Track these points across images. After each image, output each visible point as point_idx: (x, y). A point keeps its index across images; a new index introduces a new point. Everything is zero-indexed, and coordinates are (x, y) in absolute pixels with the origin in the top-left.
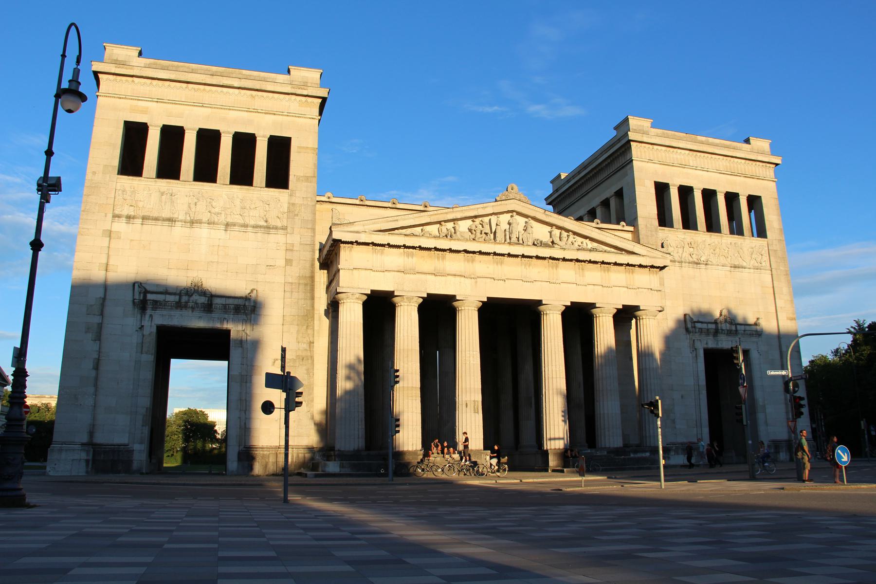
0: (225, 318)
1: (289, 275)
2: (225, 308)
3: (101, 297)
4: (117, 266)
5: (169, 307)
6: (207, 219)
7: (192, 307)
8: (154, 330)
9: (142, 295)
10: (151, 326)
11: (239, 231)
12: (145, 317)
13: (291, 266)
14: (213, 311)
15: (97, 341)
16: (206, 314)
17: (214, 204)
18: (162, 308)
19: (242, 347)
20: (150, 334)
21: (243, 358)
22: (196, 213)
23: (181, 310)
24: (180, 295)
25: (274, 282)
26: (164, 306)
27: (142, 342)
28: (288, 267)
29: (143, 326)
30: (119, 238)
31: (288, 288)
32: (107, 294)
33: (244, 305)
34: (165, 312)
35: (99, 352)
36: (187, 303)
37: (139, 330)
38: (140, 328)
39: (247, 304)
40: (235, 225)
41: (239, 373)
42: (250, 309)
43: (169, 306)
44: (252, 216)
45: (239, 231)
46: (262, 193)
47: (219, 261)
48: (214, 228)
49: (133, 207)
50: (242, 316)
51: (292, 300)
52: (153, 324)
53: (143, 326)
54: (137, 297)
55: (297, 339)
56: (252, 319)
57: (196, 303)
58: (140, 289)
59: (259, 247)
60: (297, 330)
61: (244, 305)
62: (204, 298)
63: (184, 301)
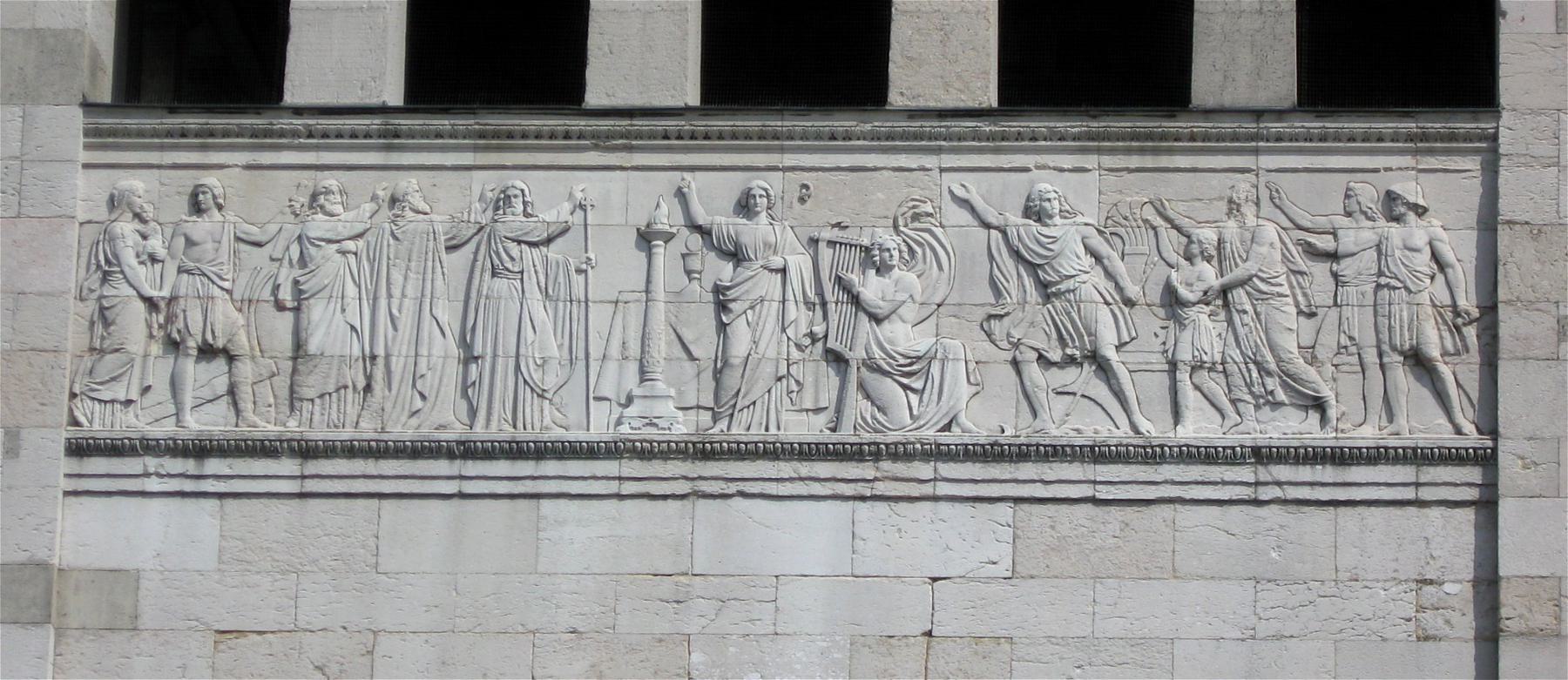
6: (821, 420)
11: (1094, 501)
17: (872, 288)
22: (732, 380)
40: (1055, 453)
44: (1196, 367)
45: (1094, 501)
46: (1267, 161)
48: (881, 488)
49: (220, 364)
59: (1263, 629)
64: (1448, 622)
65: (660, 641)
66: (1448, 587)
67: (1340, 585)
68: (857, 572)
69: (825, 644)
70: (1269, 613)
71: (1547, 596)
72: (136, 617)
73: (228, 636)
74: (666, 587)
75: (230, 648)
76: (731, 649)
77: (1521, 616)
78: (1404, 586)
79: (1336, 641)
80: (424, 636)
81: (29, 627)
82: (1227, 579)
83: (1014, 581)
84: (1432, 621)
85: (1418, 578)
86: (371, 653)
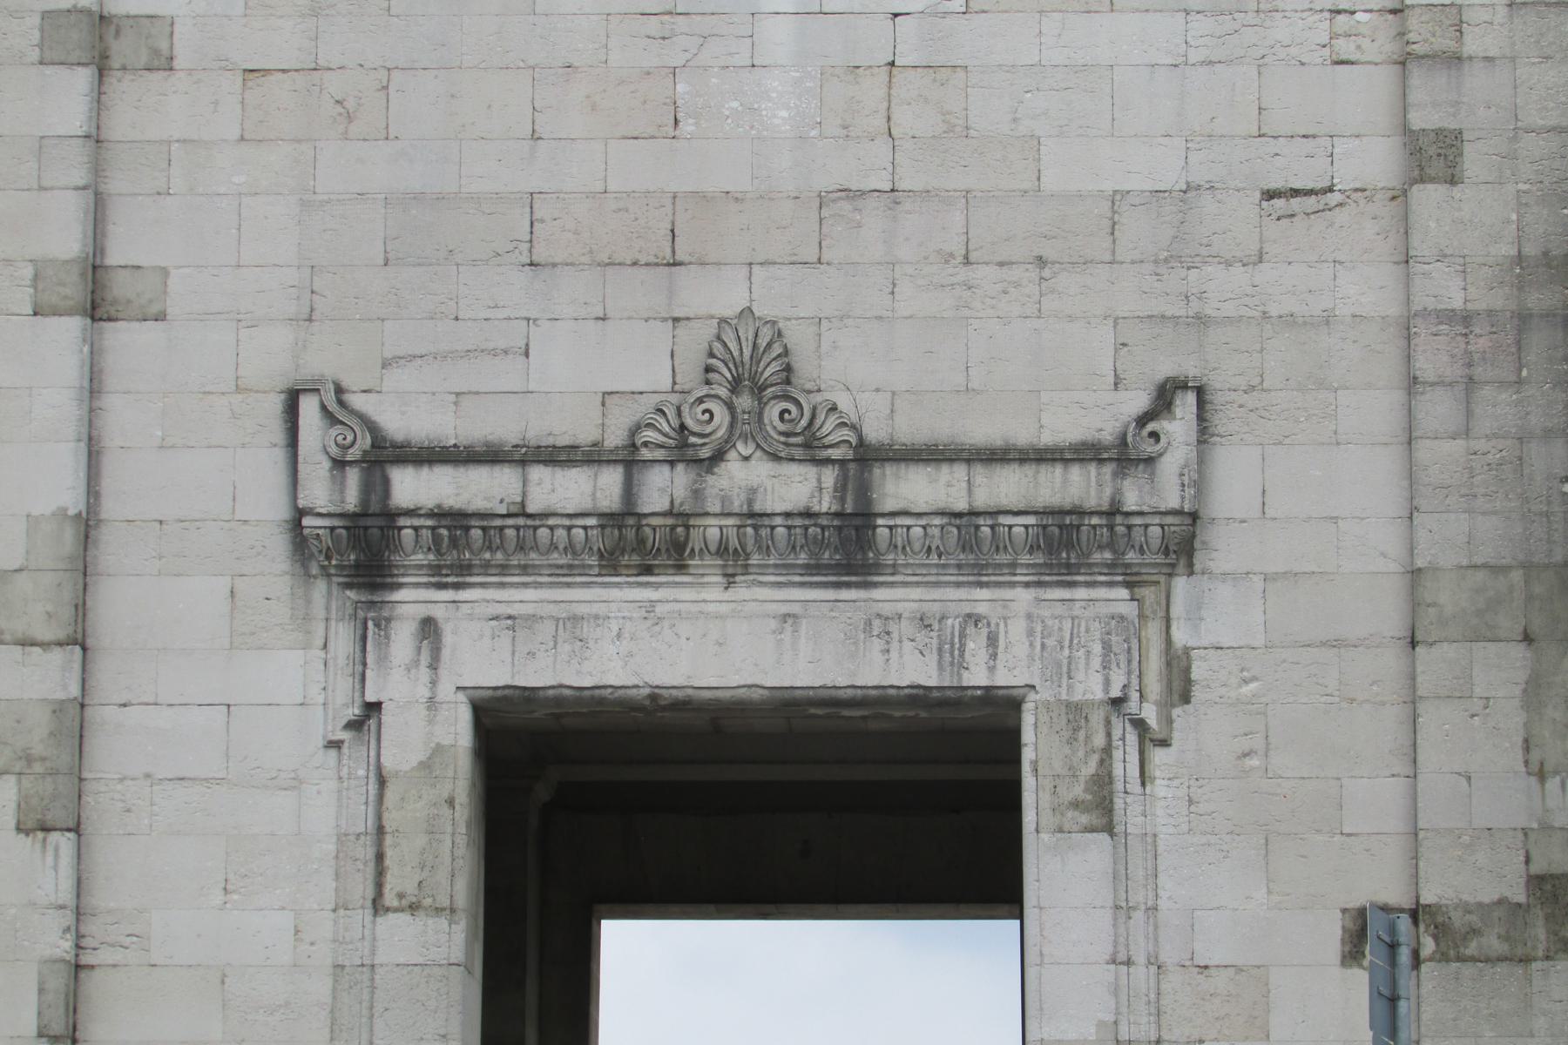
0: (974, 619)
1: (1442, 257)
2: (969, 544)
3: (61, 513)
4: (164, 272)
5: (557, 558)
7: (722, 550)
8: (459, 731)
9: (353, 477)
10: (432, 703)
12: (383, 624)
13: (1453, 181)
14: (876, 568)
15: (54, 837)
16: (830, 594)
18: (504, 569)
19: (1109, 829)
20: (425, 765)
21: (1122, 910)
23: (648, 570)
24: (630, 459)
25: (1328, 320)
26: (521, 547)
27: (380, 830)
28: (1427, 197)
29: (373, 708)
30: (164, 63)
31: (1434, 358)
32: (107, 484)
33: (1114, 511)
34: (523, 598)
35: (79, 913)
36: (681, 517)
37: (345, 736)
38: (355, 725)
39: (1131, 501)
41: (1101, 1024)
42: (1155, 531)
43: (553, 546)
47: (901, 185)
50: (1102, 593)
51: (1481, 445)
52: (446, 690)
53: (373, 708)
54: (319, 491)
55: (1527, 746)
56: (1177, 609)
57: (754, 516)
58: (334, 431)
60: (1522, 676)
61: (1114, 511)
62: (810, 471)
63: (662, 504)
64: (1359, 47)
65: (648, 73)
66: (1359, 16)
67: (1262, 15)
68: (824, 10)
69: (798, 74)
70: (1201, 41)
71: (1449, 22)
72: (172, 58)
73: (256, 74)
74: (653, 26)
75: (258, 85)
76: (713, 80)
77: (1425, 41)
78: (1317, 17)
79: (1259, 66)
80: (436, 72)
81: (75, 67)
82: (1160, 11)
83: (967, 16)
84: (1345, 48)
85: (1333, 8)
86: (386, 88)
